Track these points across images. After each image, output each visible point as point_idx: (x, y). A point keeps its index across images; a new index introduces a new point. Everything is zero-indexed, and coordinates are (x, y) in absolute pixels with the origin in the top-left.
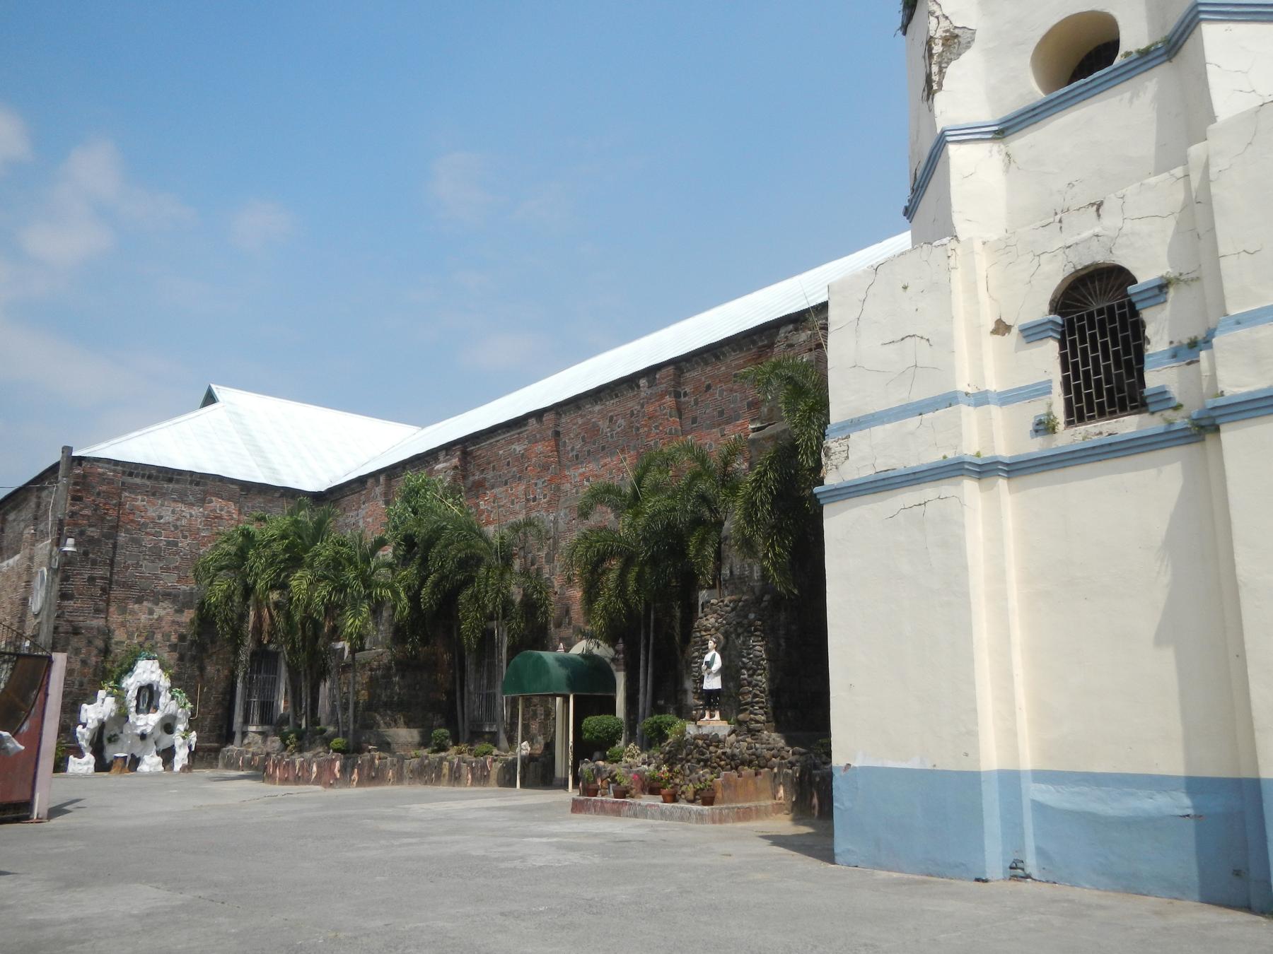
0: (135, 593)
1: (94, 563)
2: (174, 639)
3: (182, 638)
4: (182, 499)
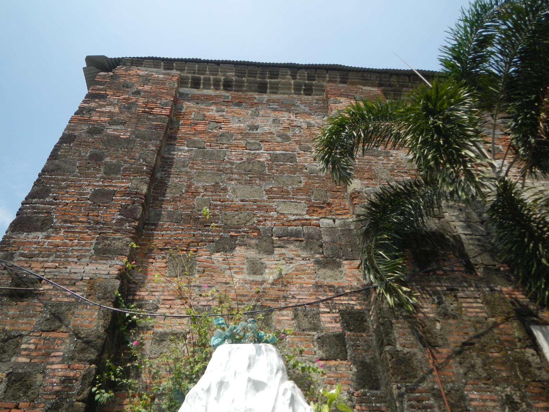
0: (214, 231)
1: (112, 171)
2: (330, 323)
3: (352, 320)
4: (288, 107)
